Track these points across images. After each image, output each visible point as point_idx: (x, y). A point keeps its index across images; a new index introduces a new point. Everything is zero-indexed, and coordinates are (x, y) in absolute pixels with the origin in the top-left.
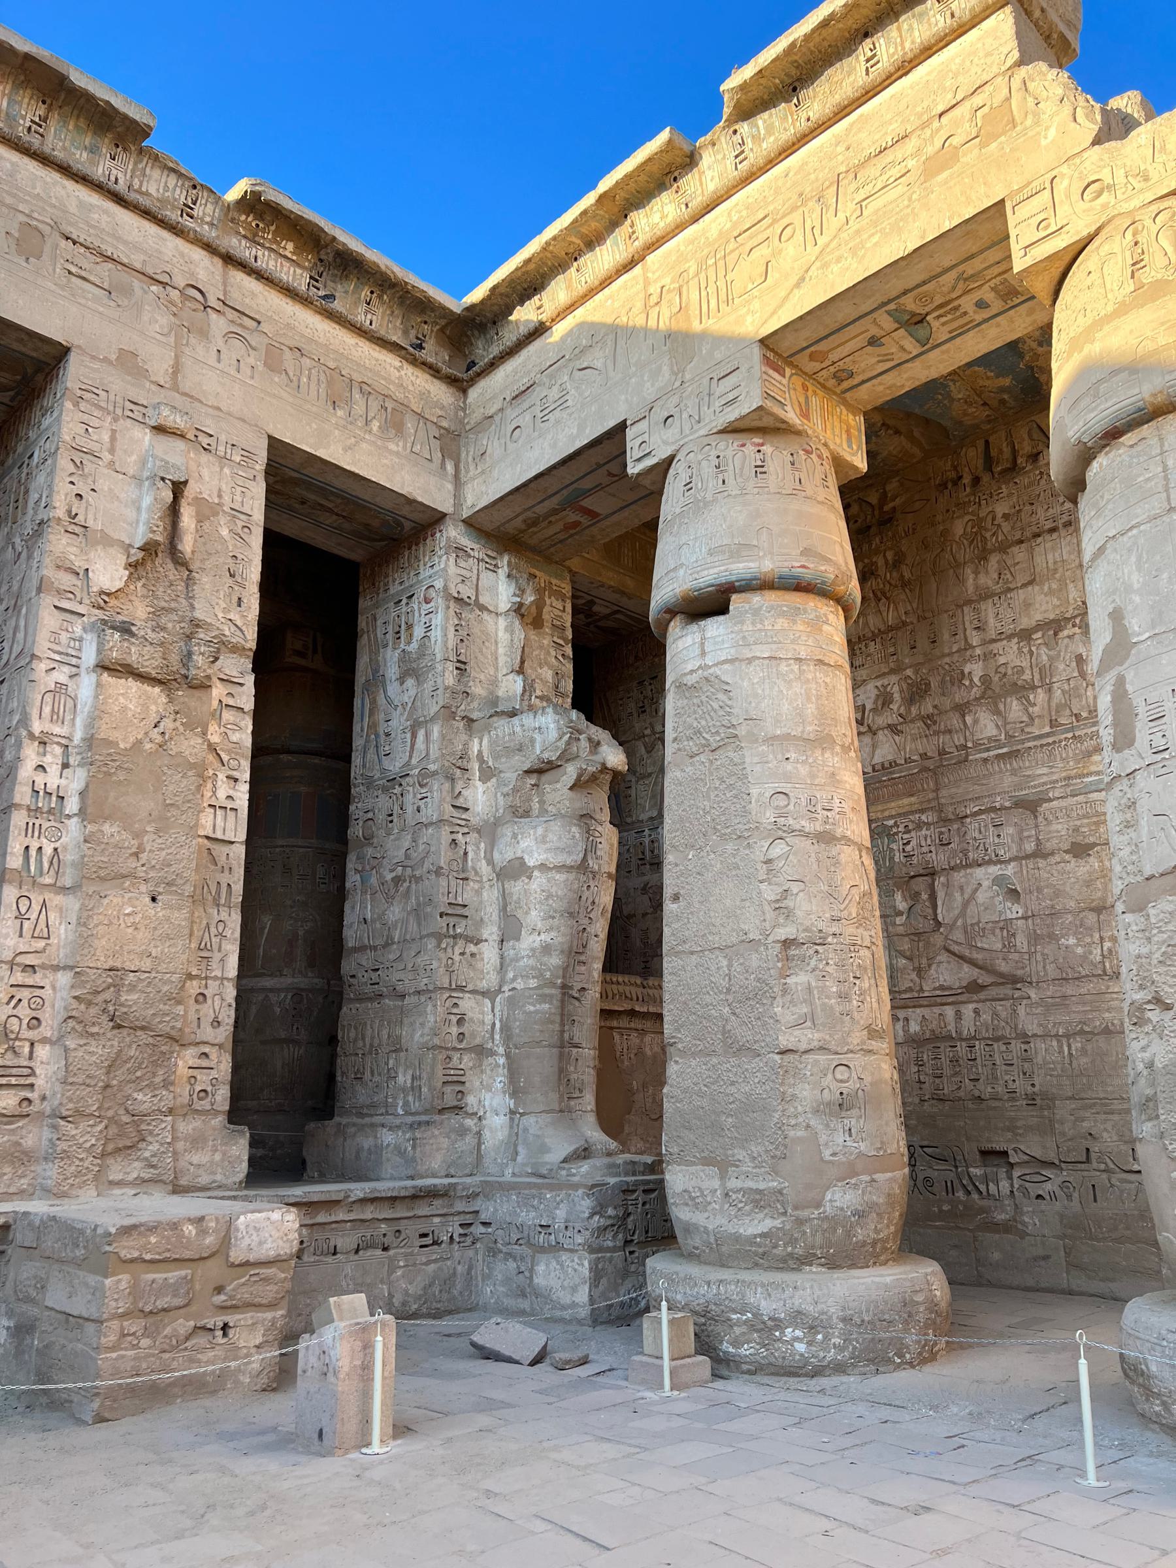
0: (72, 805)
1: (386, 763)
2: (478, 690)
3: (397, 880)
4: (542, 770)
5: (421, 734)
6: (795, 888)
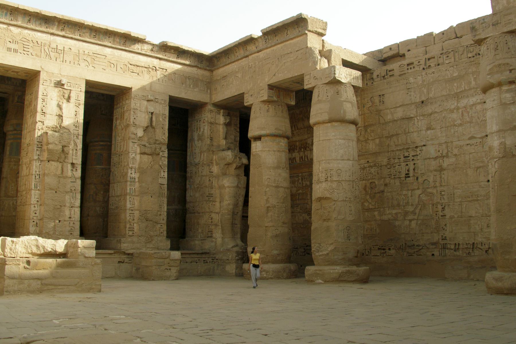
0: (137, 180)
1: (195, 160)
2: (215, 144)
3: (198, 188)
4: (228, 164)
6: (270, 197)
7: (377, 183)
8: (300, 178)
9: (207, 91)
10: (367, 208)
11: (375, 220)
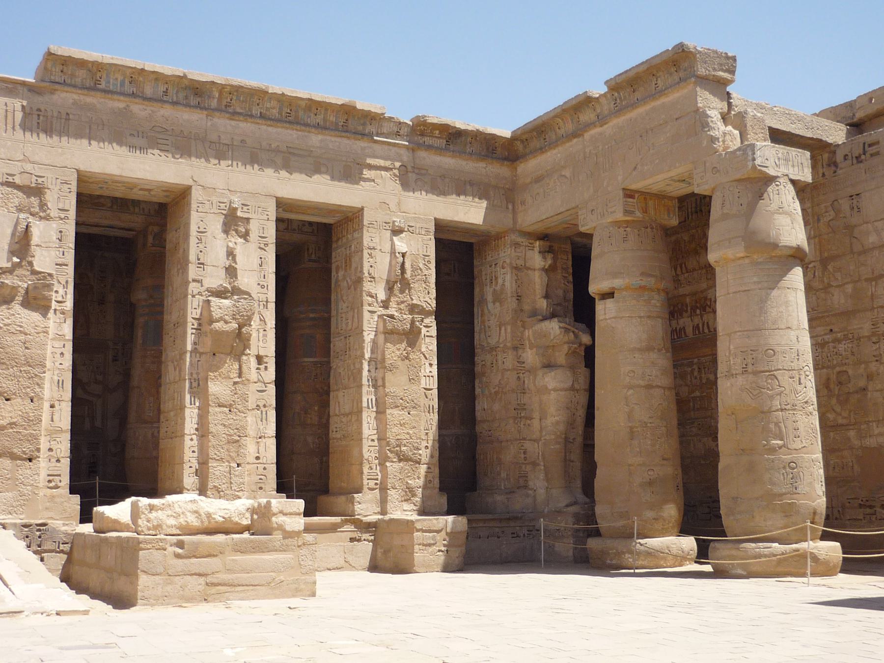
1: (489, 340)
2: (526, 307)
3: (496, 393)
5: (503, 328)
7: (850, 372)
8: (695, 367)
9: (507, 208)
10: (832, 424)
11: (851, 448)
